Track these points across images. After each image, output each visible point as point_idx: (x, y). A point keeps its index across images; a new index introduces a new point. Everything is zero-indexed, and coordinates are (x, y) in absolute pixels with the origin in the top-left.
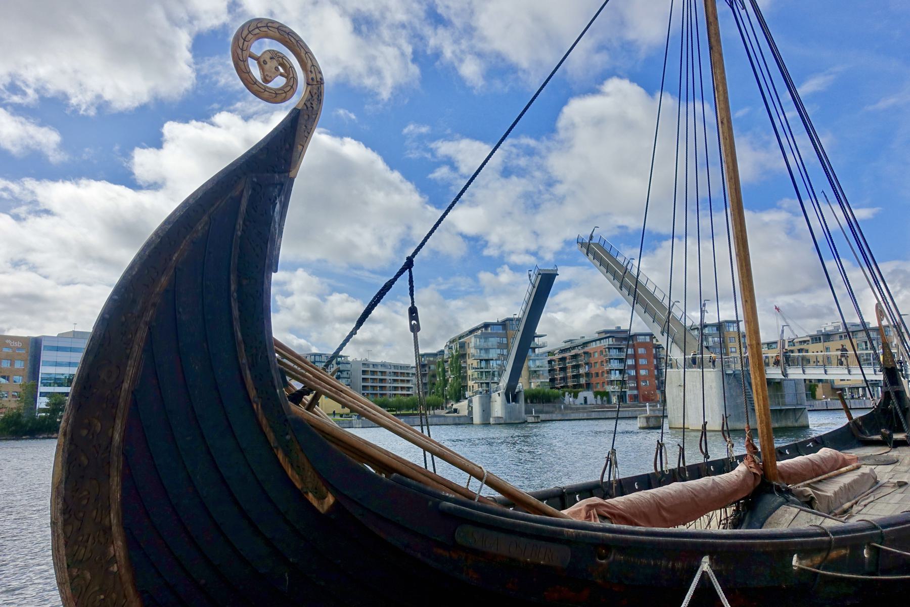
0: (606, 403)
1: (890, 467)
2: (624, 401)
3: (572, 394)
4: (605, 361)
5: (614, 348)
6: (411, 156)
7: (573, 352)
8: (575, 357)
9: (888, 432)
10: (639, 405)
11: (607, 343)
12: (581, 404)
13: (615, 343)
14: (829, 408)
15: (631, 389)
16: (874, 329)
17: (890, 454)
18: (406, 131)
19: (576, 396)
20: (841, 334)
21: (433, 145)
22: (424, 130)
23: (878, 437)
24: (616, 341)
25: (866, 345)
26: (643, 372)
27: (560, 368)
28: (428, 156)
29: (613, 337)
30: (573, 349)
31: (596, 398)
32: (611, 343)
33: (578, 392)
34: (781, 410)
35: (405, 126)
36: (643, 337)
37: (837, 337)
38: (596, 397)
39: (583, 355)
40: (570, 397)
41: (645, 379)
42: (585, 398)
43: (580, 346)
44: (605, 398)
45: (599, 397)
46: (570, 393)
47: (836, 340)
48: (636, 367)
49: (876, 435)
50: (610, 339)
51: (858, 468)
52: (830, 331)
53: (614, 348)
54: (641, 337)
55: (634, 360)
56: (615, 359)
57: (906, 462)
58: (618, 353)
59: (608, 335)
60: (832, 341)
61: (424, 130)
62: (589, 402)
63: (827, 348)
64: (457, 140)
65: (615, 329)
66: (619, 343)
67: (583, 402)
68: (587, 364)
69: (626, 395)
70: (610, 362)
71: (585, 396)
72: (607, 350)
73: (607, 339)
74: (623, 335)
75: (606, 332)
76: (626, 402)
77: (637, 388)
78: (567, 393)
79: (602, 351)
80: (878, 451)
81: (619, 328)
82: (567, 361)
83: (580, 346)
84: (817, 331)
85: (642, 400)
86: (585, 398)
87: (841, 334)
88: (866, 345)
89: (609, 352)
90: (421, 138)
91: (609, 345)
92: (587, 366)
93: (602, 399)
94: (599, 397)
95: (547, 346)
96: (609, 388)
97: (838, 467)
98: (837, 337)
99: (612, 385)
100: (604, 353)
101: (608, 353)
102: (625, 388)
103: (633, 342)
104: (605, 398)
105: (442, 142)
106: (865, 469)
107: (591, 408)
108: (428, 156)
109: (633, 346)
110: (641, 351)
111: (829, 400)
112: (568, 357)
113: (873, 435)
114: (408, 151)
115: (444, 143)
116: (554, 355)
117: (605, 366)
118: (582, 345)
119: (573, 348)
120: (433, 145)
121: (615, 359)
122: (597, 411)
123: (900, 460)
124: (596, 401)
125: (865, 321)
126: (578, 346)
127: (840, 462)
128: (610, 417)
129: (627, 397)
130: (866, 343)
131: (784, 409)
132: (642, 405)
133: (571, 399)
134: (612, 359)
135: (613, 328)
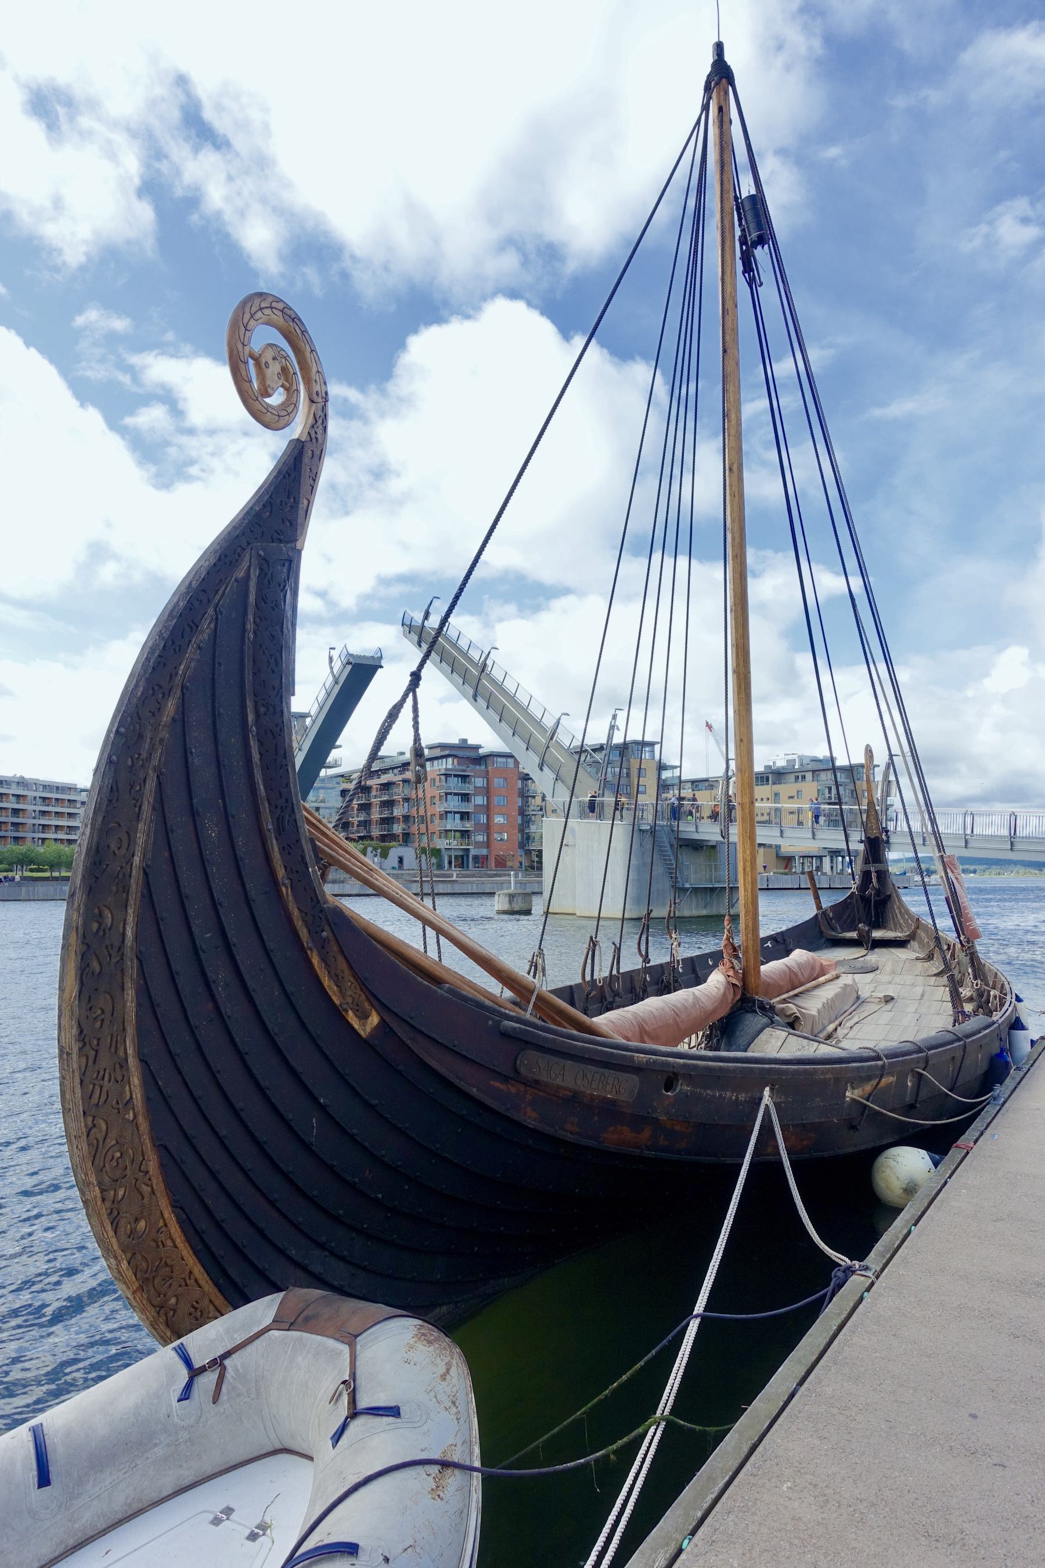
0: (435, 867)
1: (870, 976)
2: (465, 865)
3: (379, 851)
4: (437, 798)
5: (455, 776)
6: (89, 373)
7: (385, 779)
8: (387, 786)
9: (867, 928)
10: (489, 872)
11: (444, 767)
12: (393, 868)
13: (457, 767)
14: (770, 887)
15: (478, 845)
16: (843, 769)
17: (867, 958)
18: (80, 321)
19: (384, 855)
20: (797, 774)
21: (135, 360)
22: (120, 324)
23: (854, 935)
24: (459, 764)
25: (830, 792)
26: (499, 819)
27: (359, 805)
28: (126, 379)
29: (454, 756)
30: (384, 773)
32: (450, 766)
33: (389, 848)
34: (712, 890)
35: (80, 311)
36: (503, 760)
37: (792, 777)
39: (401, 785)
40: (376, 855)
41: (502, 828)
42: (401, 860)
43: (397, 768)
46: (375, 849)
47: (789, 783)
48: (487, 809)
49: (849, 931)
50: (450, 760)
51: (837, 977)
52: (783, 768)
53: (455, 776)
54: (500, 760)
55: (485, 798)
56: (455, 794)
57: (888, 969)
58: (460, 785)
59: (447, 752)
60: (784, 783)
61: (120, 324)
63: (776, 794)
64: (186, 357)
65: (457, 742)
66: (464, 768)
67: (396, 865)
68: (407, 800)
69: (468, 856)
70: (446, 800)
71: (400, 855)
72: (443, 777)
73: (444, 760)
74: (472, 754)
75: (442, 746)
76: (468, 867)
77: (488, 844)
78: (370, 849)
79: (434, 779)
80: (853, 954)
81: (465, 741)
82: (374, 793)
83: (397, 768)
84: (766, 767)
85: (493, 865)
86: (401, 860)
87: (797, 774)
88: (830, 792)
89: (446, 782)
90: (112, 339)
91: (446, 769)
92: (406, 804)
95: (340, 765)
96: (441, 844)
97: (815, 975)
98: (792, 777)
99: (446, 838)
100: (437, 784)
101: (444, 784)
102: (468, 845)
103: (486, 767)
104: (434, 860)
105: (156, 356)
106: (846, 979)
107: (409, 874)
108: (126, 379)
109: (486, 775)
110: (498, 782)
111: (772, 874)
112: (375, 787)
113: (844, 931)
114: (84, 364)
115: (160, 357)
116: (351, 782)
117: (437, 805)
118: (400, 767)
119: (385, 771)
120: (135, 360)
121: (455, 794)
123: (880, 968)
125: (834, 755)
126: (393, 769)
127: (818, 969)
128: (441, 892)
129: (471, 859)
130: (830, 789)
131: (717, 888)
132: (495, 872)
133: (376, 859)
134: (450, 794)
135: (454, 740)
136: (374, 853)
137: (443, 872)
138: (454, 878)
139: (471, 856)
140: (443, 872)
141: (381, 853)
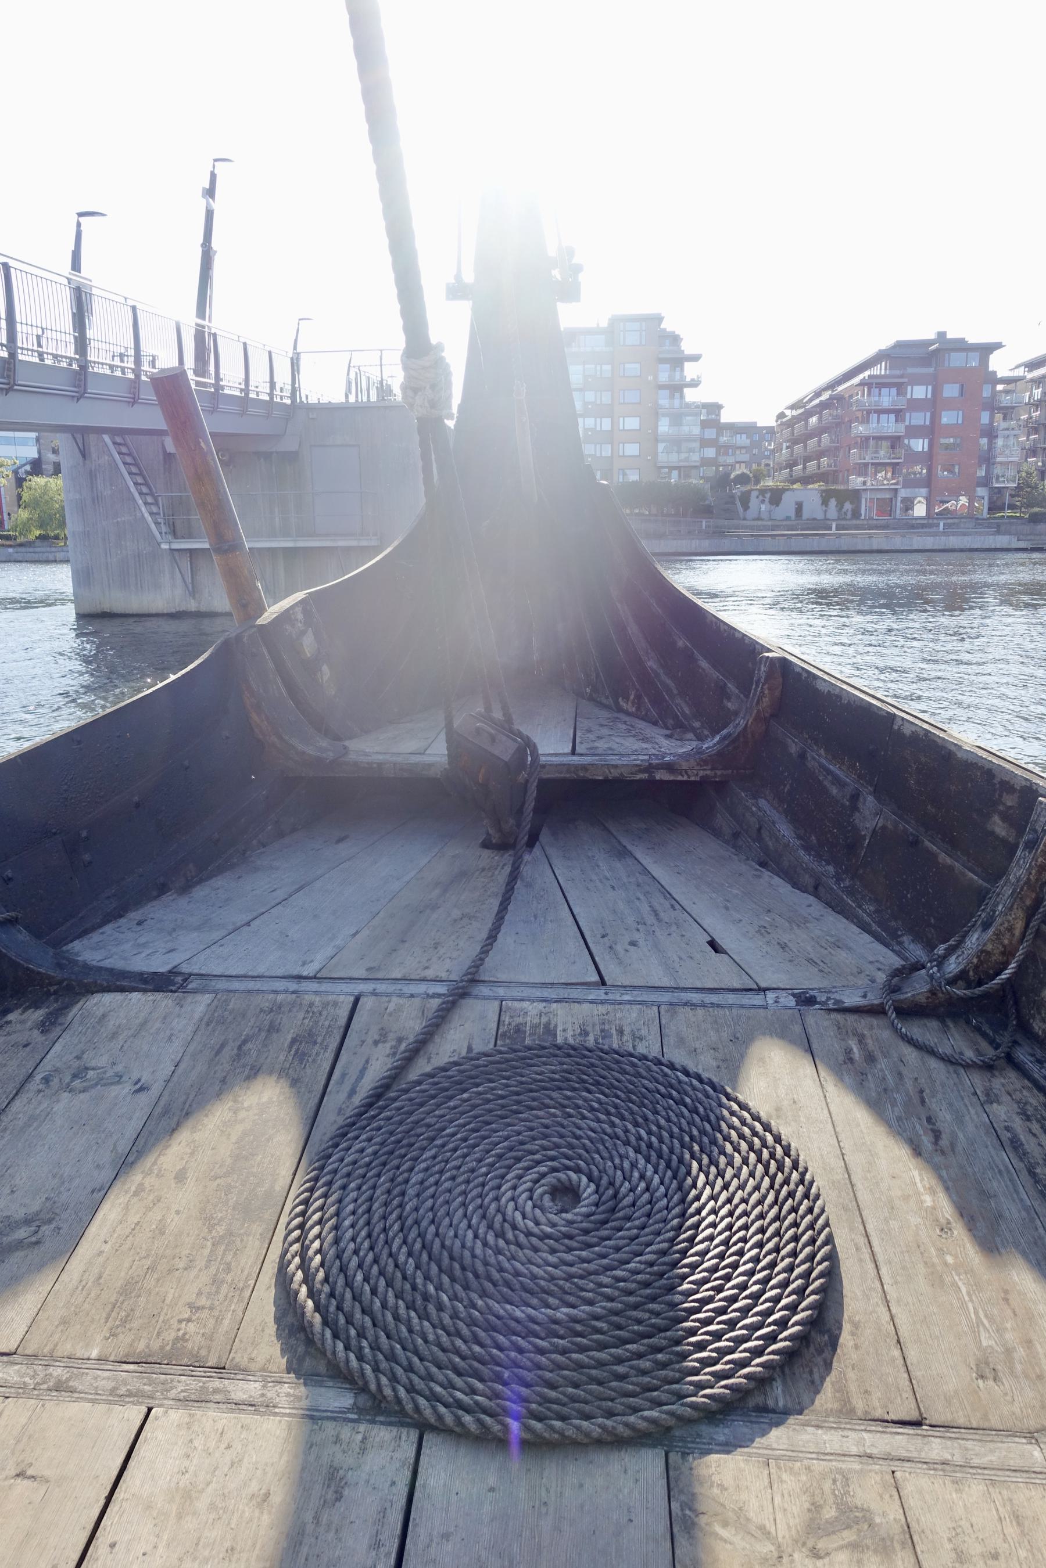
3: (768, 495)
31: (826, 506)
38: (825, 502)
40: (763, 501)
44: (848, 506)
45: (833, 502)
62: (806, 514)
67: (793, 515)
71: (799, 500)
86: (799, 508)
93: (840, 506)
94: (833, 502)
104: (848, 506)
122: (802, 535)
124: (826, 511)
133: (763, 507)
136: (761, 497)
137: (858, 522)
138: (834, 531)
139: (899, 499)
140: (858, 522)
141: (770, 498)
